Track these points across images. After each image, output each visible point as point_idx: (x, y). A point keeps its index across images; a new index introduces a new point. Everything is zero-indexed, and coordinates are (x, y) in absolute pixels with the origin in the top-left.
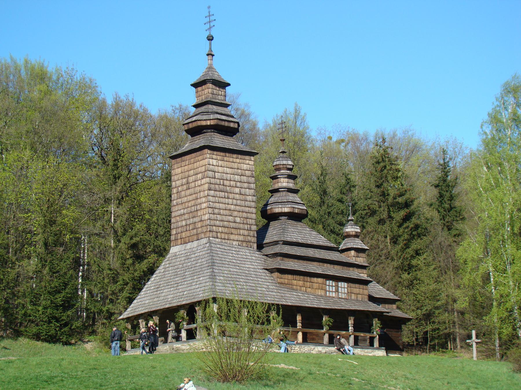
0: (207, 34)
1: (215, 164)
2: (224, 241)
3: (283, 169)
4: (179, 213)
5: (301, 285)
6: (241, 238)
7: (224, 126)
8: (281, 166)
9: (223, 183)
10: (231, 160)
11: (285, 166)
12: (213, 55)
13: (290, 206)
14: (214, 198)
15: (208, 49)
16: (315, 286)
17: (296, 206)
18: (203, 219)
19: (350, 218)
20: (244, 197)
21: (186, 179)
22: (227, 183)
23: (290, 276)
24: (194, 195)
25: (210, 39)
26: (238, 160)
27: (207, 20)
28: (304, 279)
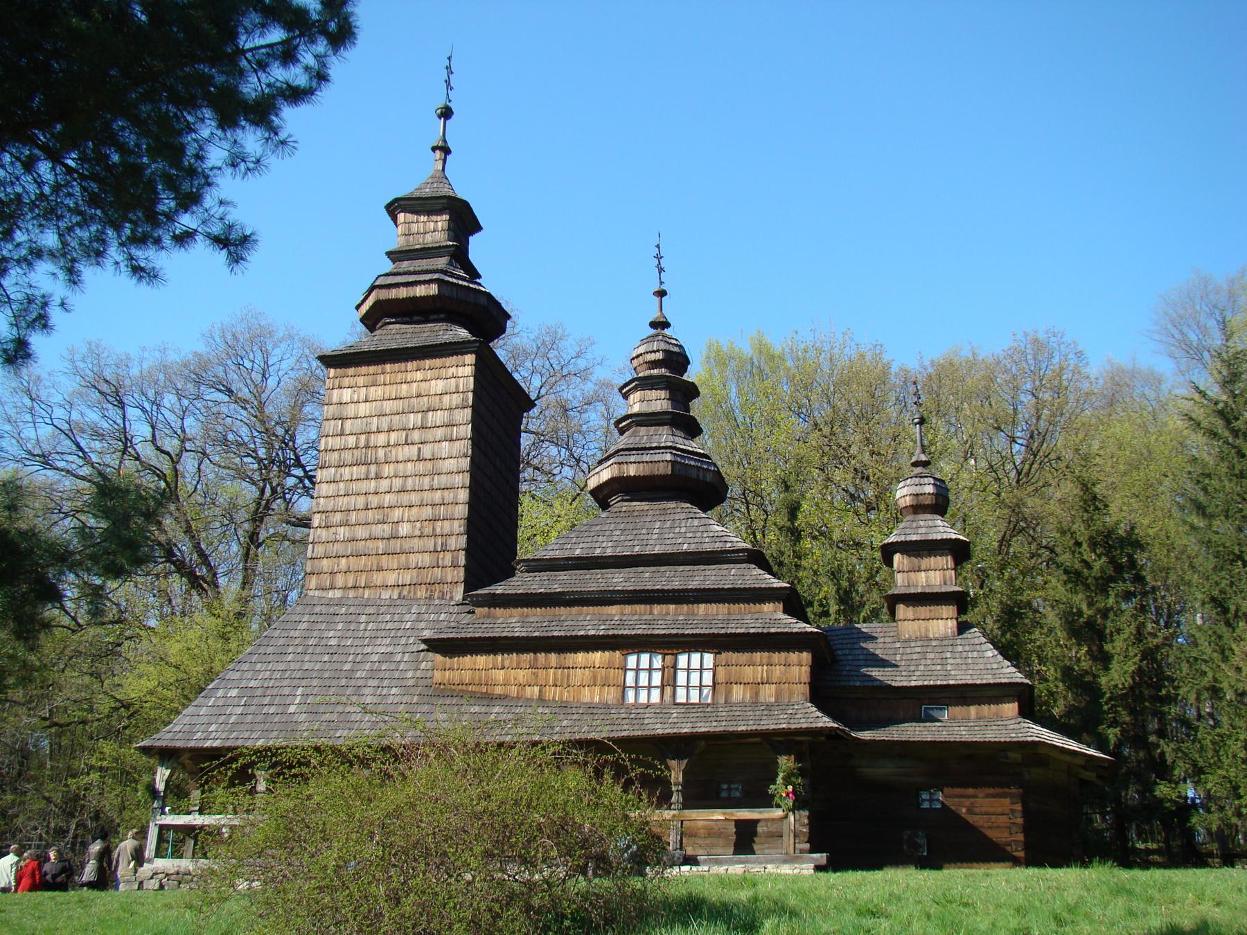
2: (352, 594)
5: (522, 680)
7: (397, 301)
14: (333, 486)
16: (578, 676)
17: (632, 459)
23: (481, 660)
25: (446, 113)
26: (419, 376)
28: (536, 659)
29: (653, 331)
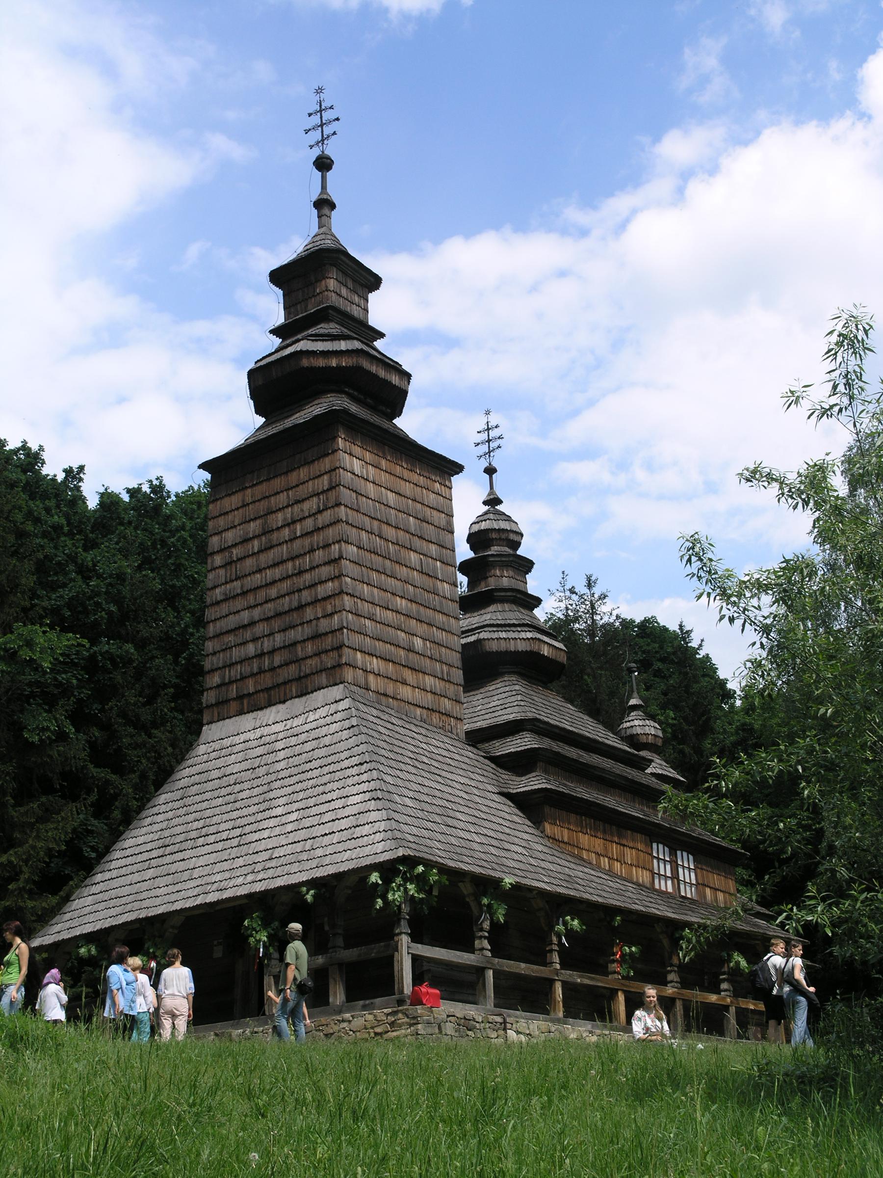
0: (316, 152)
1: (357, 470)
2: (383, 699)
4: (232, 621)
6: (428, 699)
8: (494, 535)
9: (380, 529)
10: (398, 470)
11: (503, 536)
12: (333, 206)
13: (529, 635)
15: (320, 190)
18: (322, 630)
19: (633, 702)
20: (428, 582)
21: (258, 522)
22: (390, 533)
24: (290, 565)
25: (323, 164)
29: (487, 508)
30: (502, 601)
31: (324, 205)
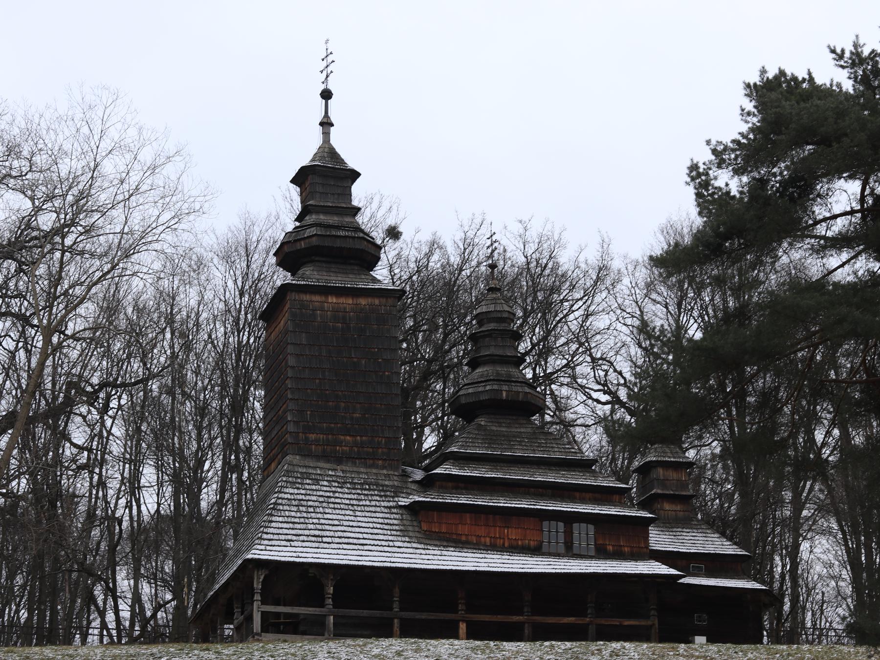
0: (323, 87)
3: (491, 320)
12: (332, 125)
13: (488, 388)
25: (326, 95)
27: (324, 64)
30: (485, 363)
31: (326, 124)
